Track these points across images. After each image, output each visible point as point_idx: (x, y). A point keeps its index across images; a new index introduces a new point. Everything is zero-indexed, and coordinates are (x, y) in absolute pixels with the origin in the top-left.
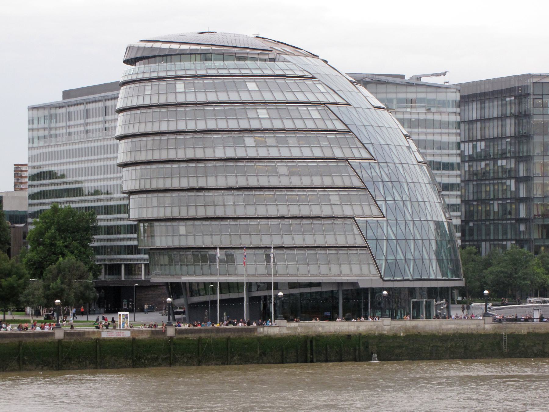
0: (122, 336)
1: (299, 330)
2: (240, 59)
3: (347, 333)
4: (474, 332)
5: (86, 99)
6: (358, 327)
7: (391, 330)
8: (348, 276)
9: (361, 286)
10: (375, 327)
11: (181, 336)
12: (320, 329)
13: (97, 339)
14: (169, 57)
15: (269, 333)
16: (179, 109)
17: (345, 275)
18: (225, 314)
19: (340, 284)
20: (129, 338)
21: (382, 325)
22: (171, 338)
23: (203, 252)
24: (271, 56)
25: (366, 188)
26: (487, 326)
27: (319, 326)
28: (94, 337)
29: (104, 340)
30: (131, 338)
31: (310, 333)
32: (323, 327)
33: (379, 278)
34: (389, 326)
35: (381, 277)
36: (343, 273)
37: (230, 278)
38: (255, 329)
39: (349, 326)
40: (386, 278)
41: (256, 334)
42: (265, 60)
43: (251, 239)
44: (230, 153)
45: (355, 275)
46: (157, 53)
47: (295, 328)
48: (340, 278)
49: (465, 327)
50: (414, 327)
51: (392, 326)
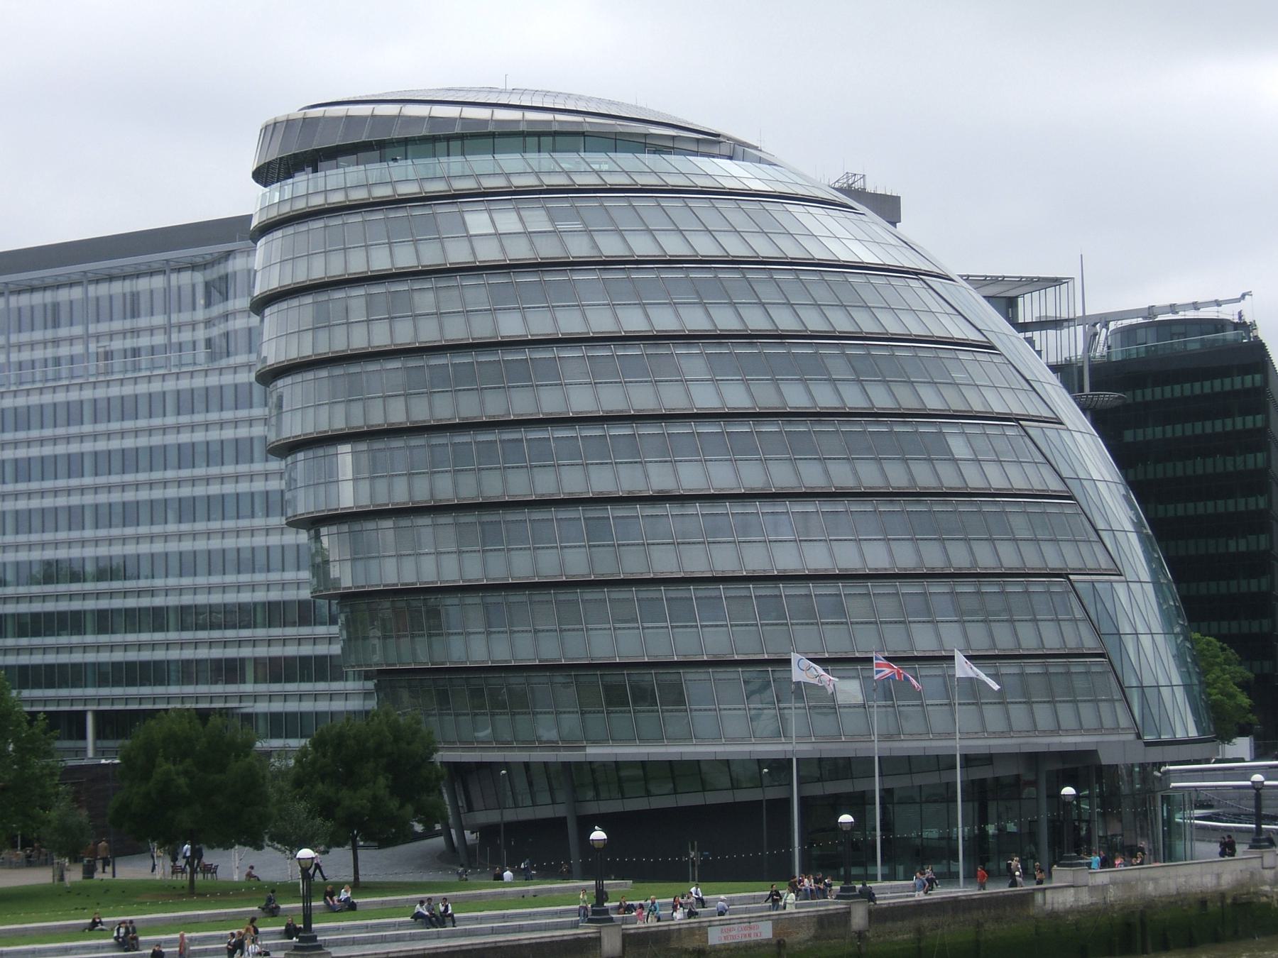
0: (753, 938)
1: (1113, 894)
2: (658, 150)
3: (1200, 896)
5: (12, 283)
6: (1219, 876)
8: (1001, 735)
9: (1105, 759)
12: (1150, 888)
14: (455, 145)
15: (1056, 906)
17: (1068, 732)
19: (1034, 759)
21: (1260, 866)
22: (860, 935)
29: (716, 950)
30: (774, 942)
32: (1155, 880)
33: (1132, 737)
34: (1273, 871)
35: (1139, 736)
38: (1026, 898)
40: (1147, 738)
41: (1032, 911)
45: (1089, 731)
46: (424, 131)
47: (1104, 887)
48: (1056, 740)
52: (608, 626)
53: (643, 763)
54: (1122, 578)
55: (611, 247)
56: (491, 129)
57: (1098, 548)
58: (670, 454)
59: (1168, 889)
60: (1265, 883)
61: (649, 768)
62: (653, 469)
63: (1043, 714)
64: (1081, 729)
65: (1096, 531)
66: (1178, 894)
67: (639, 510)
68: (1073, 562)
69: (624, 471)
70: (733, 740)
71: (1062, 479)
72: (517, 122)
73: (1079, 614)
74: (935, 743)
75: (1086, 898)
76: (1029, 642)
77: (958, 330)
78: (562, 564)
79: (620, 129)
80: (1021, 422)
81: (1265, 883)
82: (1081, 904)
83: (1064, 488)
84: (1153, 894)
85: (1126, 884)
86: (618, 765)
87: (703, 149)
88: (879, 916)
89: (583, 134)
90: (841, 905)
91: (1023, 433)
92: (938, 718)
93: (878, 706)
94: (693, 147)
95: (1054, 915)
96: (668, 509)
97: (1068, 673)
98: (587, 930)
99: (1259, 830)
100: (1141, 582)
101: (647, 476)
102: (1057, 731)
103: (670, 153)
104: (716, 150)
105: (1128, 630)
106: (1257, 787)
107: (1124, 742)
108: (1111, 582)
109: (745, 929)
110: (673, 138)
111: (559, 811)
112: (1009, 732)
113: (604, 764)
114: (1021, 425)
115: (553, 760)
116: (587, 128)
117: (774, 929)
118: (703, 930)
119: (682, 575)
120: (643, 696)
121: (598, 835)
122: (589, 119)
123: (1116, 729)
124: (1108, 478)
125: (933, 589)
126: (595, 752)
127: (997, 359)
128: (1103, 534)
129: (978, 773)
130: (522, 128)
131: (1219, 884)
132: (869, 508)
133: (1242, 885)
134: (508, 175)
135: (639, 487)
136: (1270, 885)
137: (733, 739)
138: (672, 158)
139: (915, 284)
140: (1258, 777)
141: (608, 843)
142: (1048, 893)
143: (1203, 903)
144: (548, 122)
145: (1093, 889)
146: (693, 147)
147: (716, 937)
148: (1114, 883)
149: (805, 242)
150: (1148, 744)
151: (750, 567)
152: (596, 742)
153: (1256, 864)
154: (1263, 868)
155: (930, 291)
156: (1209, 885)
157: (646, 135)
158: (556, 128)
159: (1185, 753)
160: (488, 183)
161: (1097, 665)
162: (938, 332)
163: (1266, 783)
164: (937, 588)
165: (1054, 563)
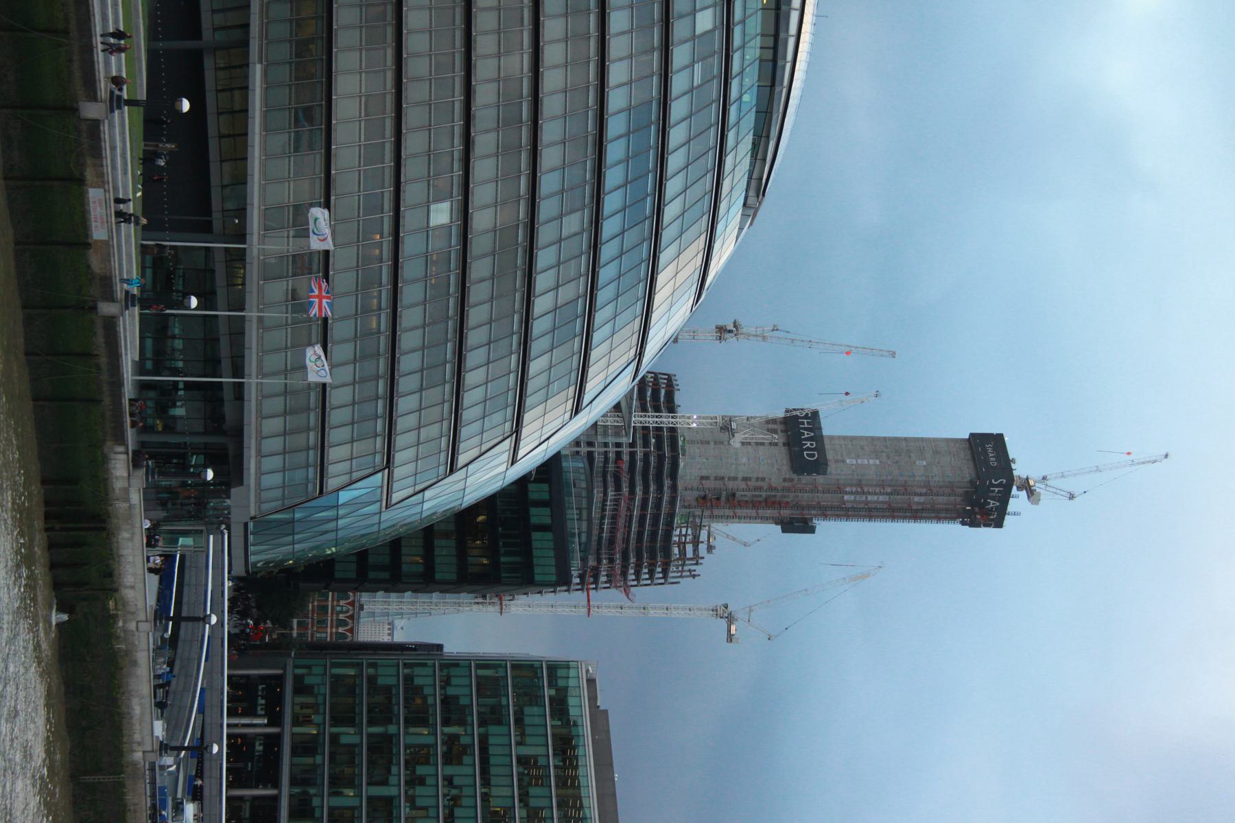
0: (93, 224)
1: (121, 506)
2: (755, 146)
4: (125, 739)
6: (132, 587)
7: (125, 631)
10: (132, 609)
11: (100, 332)
12: (125, 535)
15: (113, 462)
16: (656, 55)
18: (173, 146)
20: (92, 237)
21: (138, 620)
22: (94, 308)
23: (319, 115)
24: (751, 200)
25: (452, 471)
26: (138, 756)
27: (133, 534)
28: (89, 174)
30: (90, 241)
31: (114, 521)
32: (131, 539)
33: (253, 513)
34: (134, 629)
35: (252, 518)
36: (263, 459)
37: (256, 213)
38: (120, 439)
39: (134, 574)
41: (109, 443)
42: (747, 191)
43: (347, 294)
44: (548, 183)
47: (127, 500)
48: (253, 452)
49: (137, 727)
50: (134, 663)
51: (136, 633)
52: (362, 139)
53: (247, 111)
54: (384, 509)
55: (678, 109)
56: (783, 8)
57: (410, 491)
58: (504, 151)
59: (124, 548)
60: (125, 622)
61: (241, 135)
62: (491, 137)
63: (275, 444)
64: (260, 473)
65: (423, 490)
66: (119, 556)
67: (459, 123)
68: (398, 472)
69: (492, 112)
70: (263, 189)
71: (467, 465)
72: (787, 30)
73: (356, 475)
74: (254, 357)
75: (118, 485)
76: (335, 417)
77: (591, 387)
78: (418, 55)
79: (774, 117)
80: (515, 435)
81: (125, 622)
82: (114, 480)
83: (460, 465)
84: (120, 537)
85: (129, 517)
86: (245, 89)
87: (754, 183)
88: (110, 325)
89: (773, 85)
90: (120, 295)
91: (506, 435)
92: (275, 361)
93: (287, 317)
94: (755, 176)
95: (105, 460)
96: (458, 147)
97: (307, 466)
98: (103, 87)
99: (169, 618)
100: (380, 523)
101: (487, 131)
102: (260, 455)
103: (752, 157)
104: (752, 193)
105: (341, 512)
106: (205, 619)
107: (249, 507)
108: (381, 501)
109: (102, 218)
110: (764, 160)
111: (207, 34)
112: (261, 416)
113: (246, 77)
114: (513, 434)
115: (252, 35)
116: (777, 89)
117: (102, 241)
118: (101, 182)
119: (403, 156)
120: (304, 115)
121: (186, 106)
122: (785, 91)
123: (260, 501)
124: (466, 499)
125: (382, 362)
126: (257, 71)
127: (568, 415)
128: (420, 495)
129: (228, 395)
130: (782, 35)
131: (126, 587)
132: (451, 312)
133: (124, 605)
134: (743, 22)
135: (478, 125)
136: (123, 627)
137: (265, 190)
138: (747, 160)
139: (632, 352)
140: (214, 619)
141: (179, 113)
142: (124, 457)
144: (785, 57)
145: (126, 491)
146: (755, 176)
148: (131, 507)
149: (671, 269)
150: (246, 525)
151: (406, 239)
152: (265, 73)
153: (142, 616)
154: (138, 622)
155: (626, 364)
156: (125, 580)
157: (768, 137)
158: (780, 63)
159: (238, 552)
160: (737, 32)
161: (313, 488)
162: (592, 371)
163: (207, 626)
164: (383, 364)
165: (399, 457)
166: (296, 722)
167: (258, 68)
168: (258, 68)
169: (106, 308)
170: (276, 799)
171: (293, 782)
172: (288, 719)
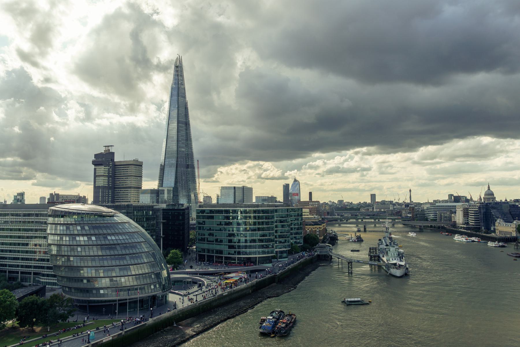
13: (102, 344)
22: (123, 335)
28: (102, 342)
32: (162, 317)
38: (146, 324)
57: (158, 268)
88: (126, 332)
95: (149, 325)
123: (159, 291)
126: (91, 299)
143: (168, 318)
147: (104, 341)
152: (92, 297)
166: (205, 252)
167: (90, 298)
168: (90, 298)
169: (123, 333)
170: (216, 256)
171: (213, 253)
172: (204, 254)
